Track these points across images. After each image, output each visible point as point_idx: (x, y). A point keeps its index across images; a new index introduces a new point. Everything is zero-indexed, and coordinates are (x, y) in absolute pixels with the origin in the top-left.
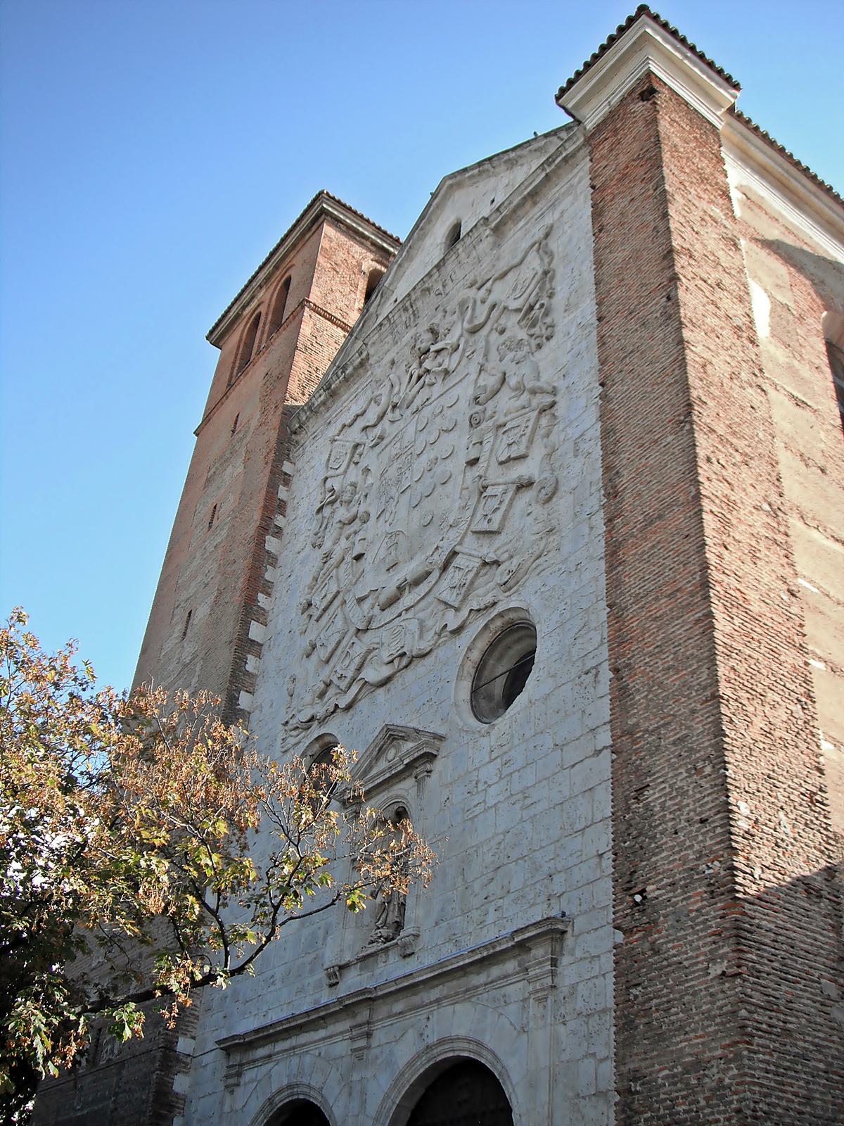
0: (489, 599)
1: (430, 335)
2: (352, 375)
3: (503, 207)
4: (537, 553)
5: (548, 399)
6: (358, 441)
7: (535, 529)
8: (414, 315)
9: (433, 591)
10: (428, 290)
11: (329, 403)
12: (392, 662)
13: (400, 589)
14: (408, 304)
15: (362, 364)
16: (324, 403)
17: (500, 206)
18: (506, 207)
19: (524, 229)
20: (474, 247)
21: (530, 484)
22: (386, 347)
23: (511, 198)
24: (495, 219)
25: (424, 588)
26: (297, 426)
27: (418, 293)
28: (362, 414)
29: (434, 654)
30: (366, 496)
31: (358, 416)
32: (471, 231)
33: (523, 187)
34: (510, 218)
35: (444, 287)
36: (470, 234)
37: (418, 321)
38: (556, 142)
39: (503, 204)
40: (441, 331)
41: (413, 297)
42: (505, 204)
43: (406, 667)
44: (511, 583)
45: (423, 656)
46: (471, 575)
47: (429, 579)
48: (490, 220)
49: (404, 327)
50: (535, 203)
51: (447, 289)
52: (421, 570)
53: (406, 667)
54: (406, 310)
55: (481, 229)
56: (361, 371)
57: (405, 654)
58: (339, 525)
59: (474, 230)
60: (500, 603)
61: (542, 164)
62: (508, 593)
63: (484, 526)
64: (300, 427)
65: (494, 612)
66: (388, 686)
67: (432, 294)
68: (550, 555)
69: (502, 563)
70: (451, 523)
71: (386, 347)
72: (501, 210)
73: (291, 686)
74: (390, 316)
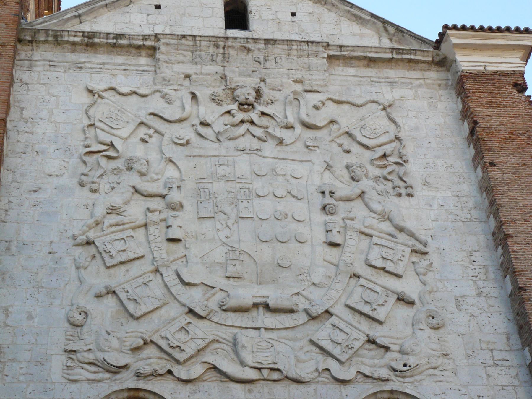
0: (384, 373)
1: (254, 94)
2: (122, 46)
3: (345, 48)
4: (434, 365)
5: (419, 247)
6: (145, 120)
7: (434, 346)
8: (224, 57)
9: (297, 329)
10: (249, 50)
11: (78, 47)
12: (259, 369)
13: (256, 305)
14: (221, 44)
15: (139, 47)
16: (74, 44)
17: (344, 46)
18: (347, 51)
19: (357, 79)
20: (308, 55)
21: (411, 303)
22: (181, 58)
23: (355, 49)
24: (333, 50)
25: (286, 320)
26: (28, 38)
27: (237, 45)
28: (142, 96)
29: (313, 386)
30: (179, 187)
31: (135, 93)
32: (312, 42)
33: (369, 50)
34: (344, 59)
35: (266, 60)
36: (310, 44)
37: (226, 64)
38: (416, 46)
39: (347, 46)
40: (265, 98)
41: (229, 43)
42: (349, 48)
43: (274, 381)
44: (407, 373)
45: (297, 381)
46: (357, 345)
47: (294, 316)
48: (330, 48)
49: (209, 57)
50: (368, 66)
51: (268, 64)
52: (287, 304)
53: (274, 381)
54: (217, 46)
55: (321, 49)
56: (134, 51)
57: (278, 370)
58: (132, 190)
59: (314, 44)
60: (392, 383)
61: (393, 49)
62: (402, 380)
63: (366, 309)
64: (31, 42)
65: (387, 387)
66: (248, 386)
67: (250, 56)
68: (445, 373)
69: (390, 351)
70: (316, 281)
71: (181, 58)
72: (343, 48)
73: (79, 318)
74: (198, 38)
